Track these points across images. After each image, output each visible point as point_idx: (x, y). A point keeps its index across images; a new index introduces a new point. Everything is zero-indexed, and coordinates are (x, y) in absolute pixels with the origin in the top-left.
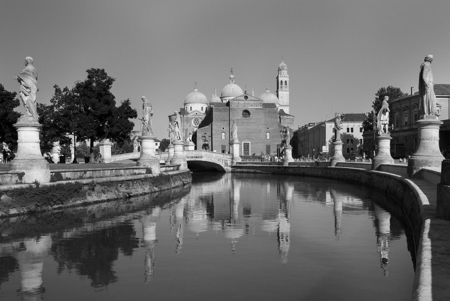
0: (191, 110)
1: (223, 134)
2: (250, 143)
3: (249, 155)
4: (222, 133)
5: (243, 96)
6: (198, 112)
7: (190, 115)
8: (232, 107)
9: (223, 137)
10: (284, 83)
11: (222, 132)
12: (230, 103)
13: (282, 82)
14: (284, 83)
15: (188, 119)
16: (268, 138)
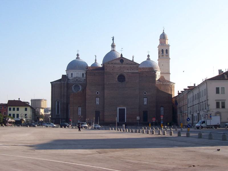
0: (72, 76)
1: (98, 99)
2: (125, 108)
3: (125, 121)
6: (79, 78)
8: (107, 71)
9: (98, 103)
10: (165, 52)
13: (163, 51)
14: (165, 52)
16: (145, 103)
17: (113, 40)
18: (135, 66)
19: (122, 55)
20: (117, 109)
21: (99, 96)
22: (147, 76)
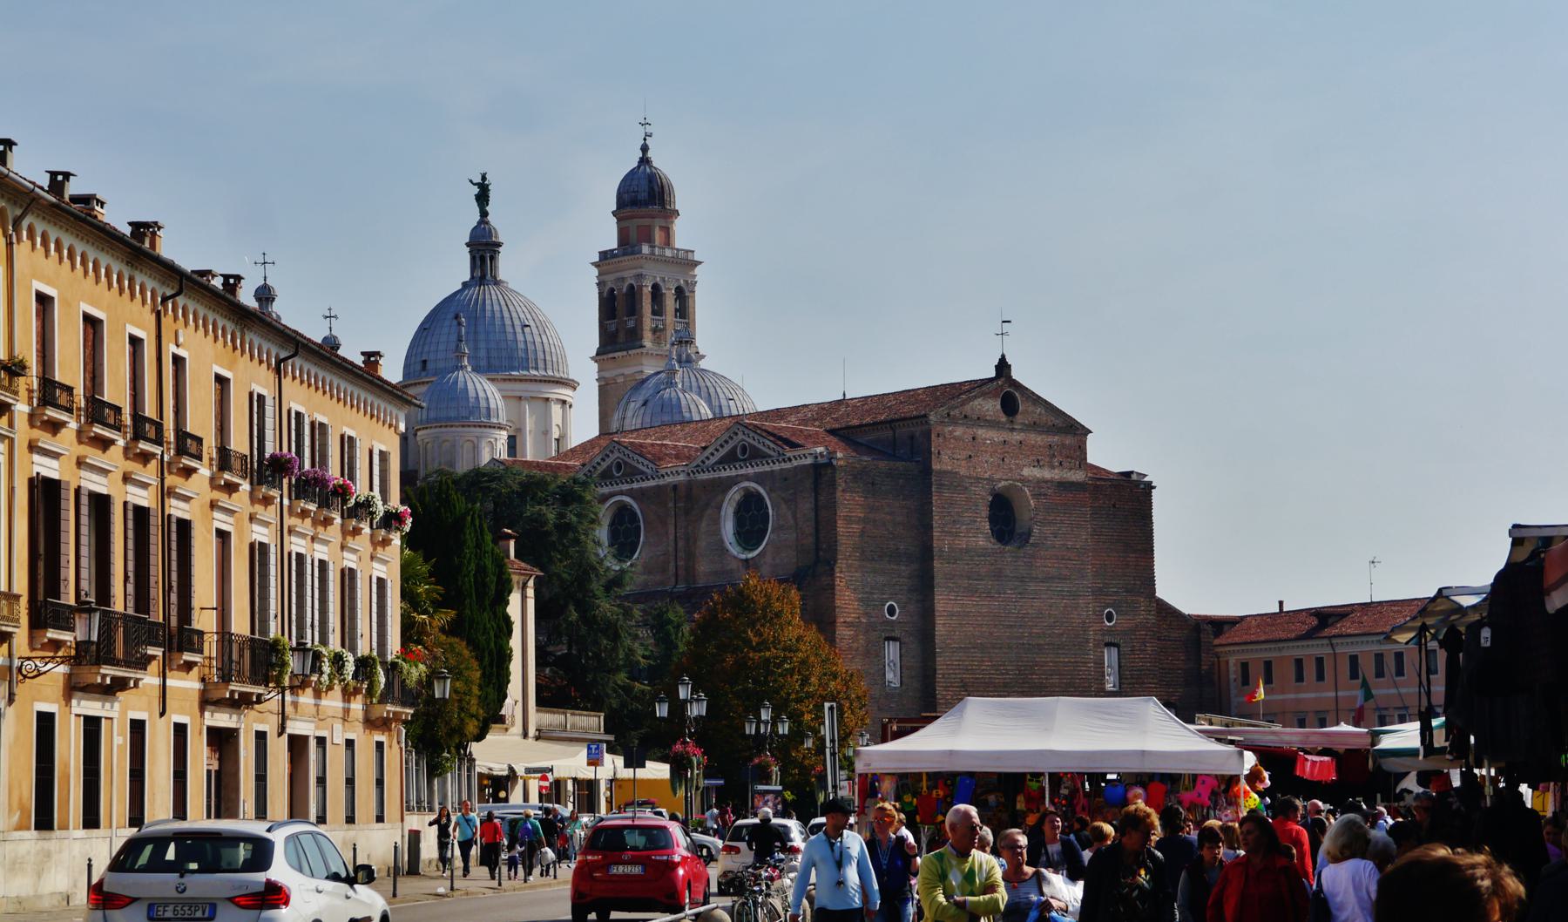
5: (995, 396)
8: (944, 468)
9: (892, 677)
10: (670, 303)
12: (933, 437)
14: (670, 303)
17: (483, 197)
18: (1069, 440)
19: (1003, 366)
21: (897, 634)
22: (1114, 506)
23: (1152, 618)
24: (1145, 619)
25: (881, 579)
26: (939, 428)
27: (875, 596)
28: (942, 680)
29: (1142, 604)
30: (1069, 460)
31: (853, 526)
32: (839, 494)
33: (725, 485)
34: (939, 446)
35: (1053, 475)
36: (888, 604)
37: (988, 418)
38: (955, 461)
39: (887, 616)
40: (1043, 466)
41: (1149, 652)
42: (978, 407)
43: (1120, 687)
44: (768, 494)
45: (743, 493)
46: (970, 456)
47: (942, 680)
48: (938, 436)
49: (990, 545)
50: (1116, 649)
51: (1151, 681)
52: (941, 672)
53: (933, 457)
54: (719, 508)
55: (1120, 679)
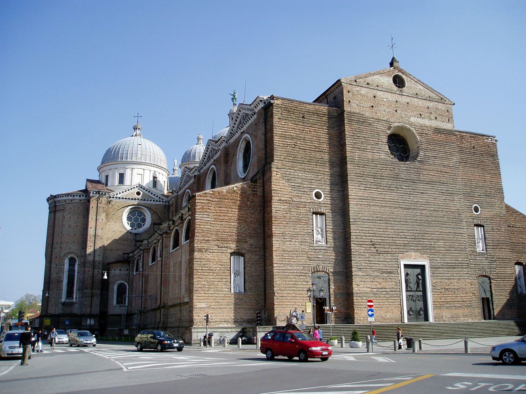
4: (314, 215)
5: (389, 75)
7: (119, 196)
8: (353, 110)
11: (313, 213)
12: (345, 92)
15: (110, 206)
16: (480, 247)
20: (399, 267)
21: (323, 210)
22: (474, 147)
23: (504, 212)
24: (499, 212)
25: (309, 176)
26: (349, 87)
27: (305, 186)
28: (356, 240)
29: (496, 203)
30: (442, 117)
31: (287, 141)
32: (276, 120)
33: (236, 143)
34: (349, 97)
35: (431, 124)
36: (315, 191)
37: (384, 87)
38: (362, 108)
39: (315, 199)
40: (424, 118)
41: (503, 231)
42: (378, 80)
43: (486, 251)
44: (251, 137)
45: (245, 143)
46: (372, 106)
47: (356, 240)
48: (349, 92)
49: (389, 159)
50: (482, 228)
51: (506, 247)
52: (355, 234)
53: (345, 103)
54: (236, 155)
55: (486, 245)
